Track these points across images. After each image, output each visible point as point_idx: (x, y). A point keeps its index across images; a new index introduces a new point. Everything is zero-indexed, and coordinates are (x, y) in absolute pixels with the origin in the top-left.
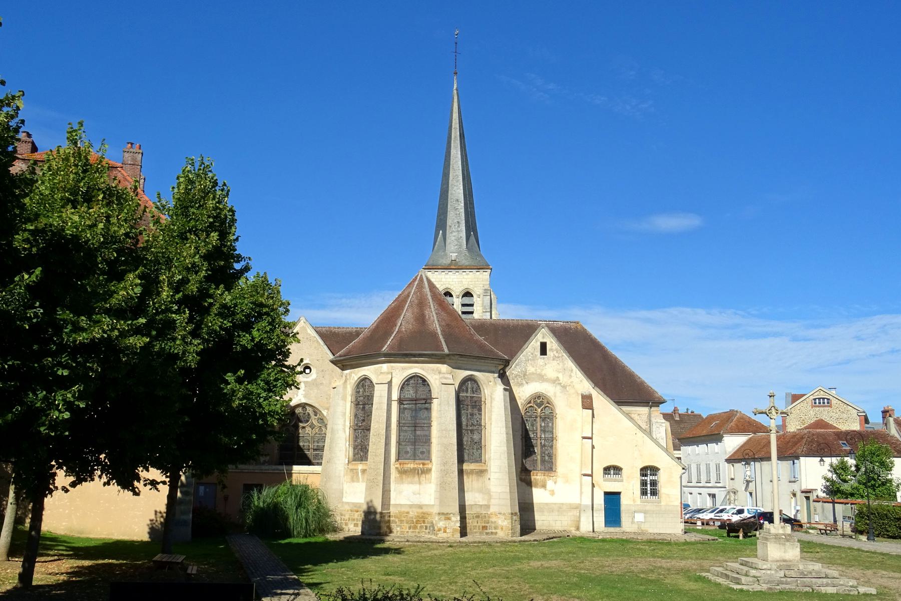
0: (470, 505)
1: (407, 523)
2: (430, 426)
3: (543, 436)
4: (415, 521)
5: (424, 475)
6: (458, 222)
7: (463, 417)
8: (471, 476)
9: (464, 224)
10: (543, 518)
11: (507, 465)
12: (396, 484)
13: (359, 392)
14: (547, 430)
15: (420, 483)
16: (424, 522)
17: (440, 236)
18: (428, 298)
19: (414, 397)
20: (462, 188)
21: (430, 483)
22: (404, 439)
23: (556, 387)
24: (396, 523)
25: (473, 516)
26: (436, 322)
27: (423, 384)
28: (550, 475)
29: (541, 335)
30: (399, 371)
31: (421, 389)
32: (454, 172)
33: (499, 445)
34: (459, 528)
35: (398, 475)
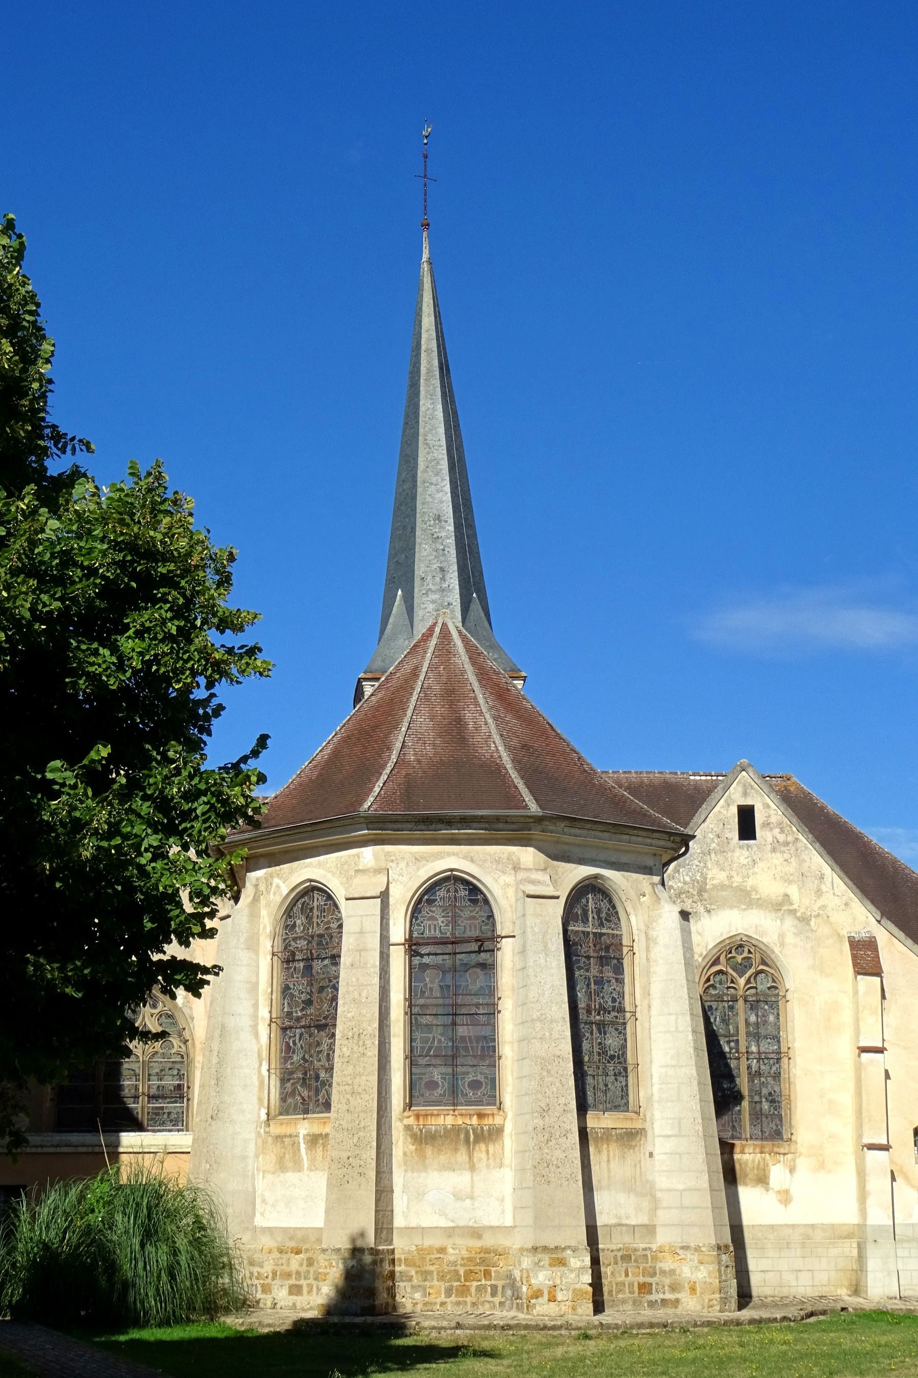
0: (607, 1226)
1: (442, 1278)
2: (492, 1012)
3: (754, 1049)
4: (462, 1273)
5: (483, 1146)
6: (442, 569)
7: (578, 989)
8: (605, 1146)
9: (456, 574)
10: (764, 1264)
11: (698, 1115)
12: (406, 1171)
13: (294, 926)
14: (762, 1031)
15: (472, 1168)
16: (487, 1274)
17: (397, 603)
18: (467, 679)
19: (448, 934)
20: (448, 488)
21: (501, 1166)
22: (422, 1048)
23: (782, 920)
24: (410, 1279)
25: (615, 1257)
26: (496, 737)
27: (470, 900)
28: (776, 1150)
29: (740, 789)
30: (408, 865)
31: (467, 913)
32: (428, 453)
33: (674, 1063)
34: (590, 1289)
35: (413, 1148)
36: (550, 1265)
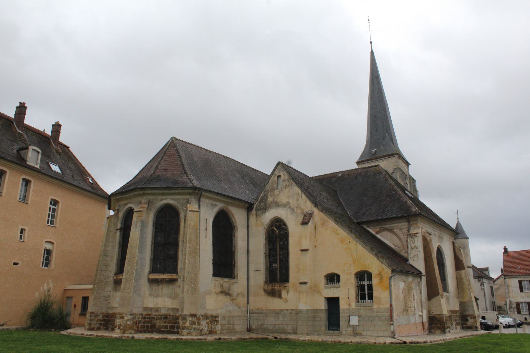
36: (120, 318)
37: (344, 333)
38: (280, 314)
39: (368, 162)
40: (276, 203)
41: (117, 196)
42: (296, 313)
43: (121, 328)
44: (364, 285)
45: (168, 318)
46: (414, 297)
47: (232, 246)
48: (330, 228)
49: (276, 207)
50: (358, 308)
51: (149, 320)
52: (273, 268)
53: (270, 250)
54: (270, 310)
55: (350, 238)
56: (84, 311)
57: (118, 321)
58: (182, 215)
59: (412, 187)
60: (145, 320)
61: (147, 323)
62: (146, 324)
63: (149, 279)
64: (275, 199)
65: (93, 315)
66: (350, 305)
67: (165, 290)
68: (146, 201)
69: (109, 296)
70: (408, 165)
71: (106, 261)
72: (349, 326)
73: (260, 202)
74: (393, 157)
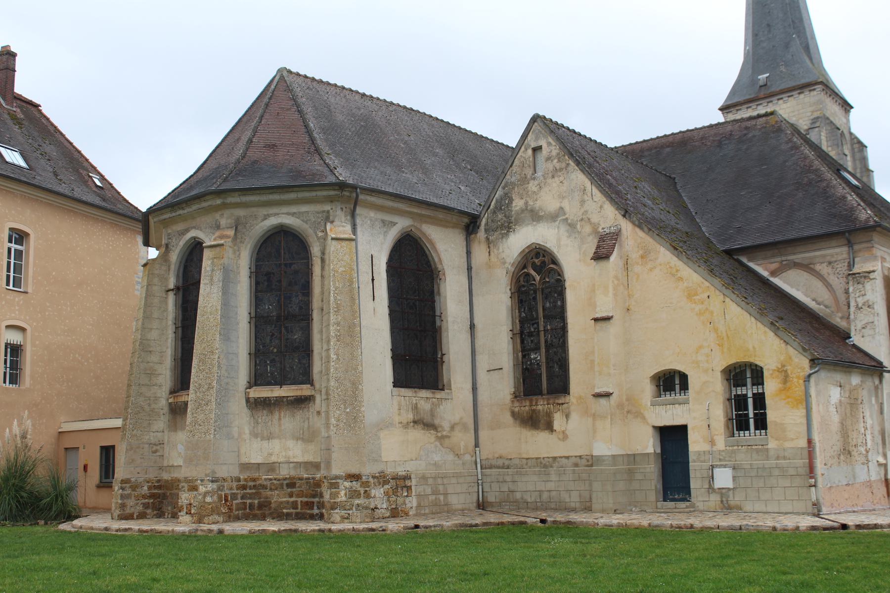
28: (557, 401)
36: (188, 490)
37: (700, 506)
38: (552, 467)
39: (780, 97)
40: (532, 211)
41: (162, 214)
42: (587, 463)
43: (193, 512)
44: (745, 397)
45: (297, 485)
46: (864, 422)
47: (434, 316)
48: (660, 265)
49: (533, 221)
50: (731, 448)
51: (254, 491)
52: (531, 363)
53: (522, 322)
54: (527, 459)
55: (708, 287)
56: (105, 479)
57: (185, 497)
58: (315, 250)
59: (858, 162)
60: (245, 491)
61: (250, 498)
62: (248, 501)
63: (248, 400)
64: (531, 203)
65: (128, 485)
66: (712, 443)
67: (288, 421)
68: (229, 221)
69: (161, 442)
70: (848, 108)
71: (148, 362)
72: (711, 491)
73: (494, 212)
74: (810, 91)
